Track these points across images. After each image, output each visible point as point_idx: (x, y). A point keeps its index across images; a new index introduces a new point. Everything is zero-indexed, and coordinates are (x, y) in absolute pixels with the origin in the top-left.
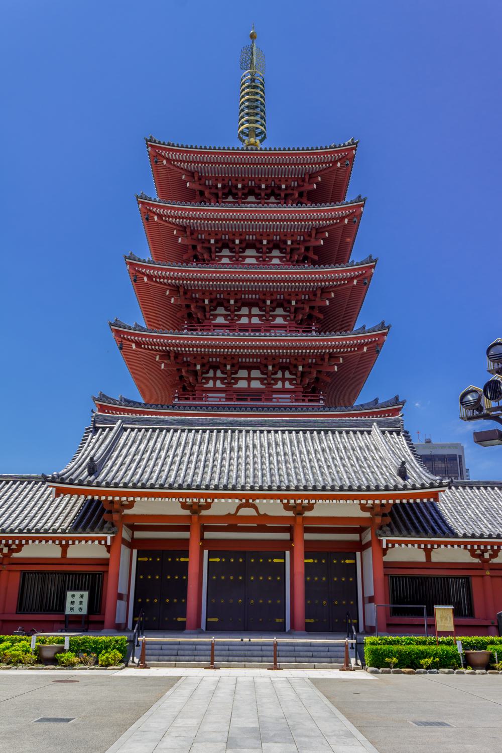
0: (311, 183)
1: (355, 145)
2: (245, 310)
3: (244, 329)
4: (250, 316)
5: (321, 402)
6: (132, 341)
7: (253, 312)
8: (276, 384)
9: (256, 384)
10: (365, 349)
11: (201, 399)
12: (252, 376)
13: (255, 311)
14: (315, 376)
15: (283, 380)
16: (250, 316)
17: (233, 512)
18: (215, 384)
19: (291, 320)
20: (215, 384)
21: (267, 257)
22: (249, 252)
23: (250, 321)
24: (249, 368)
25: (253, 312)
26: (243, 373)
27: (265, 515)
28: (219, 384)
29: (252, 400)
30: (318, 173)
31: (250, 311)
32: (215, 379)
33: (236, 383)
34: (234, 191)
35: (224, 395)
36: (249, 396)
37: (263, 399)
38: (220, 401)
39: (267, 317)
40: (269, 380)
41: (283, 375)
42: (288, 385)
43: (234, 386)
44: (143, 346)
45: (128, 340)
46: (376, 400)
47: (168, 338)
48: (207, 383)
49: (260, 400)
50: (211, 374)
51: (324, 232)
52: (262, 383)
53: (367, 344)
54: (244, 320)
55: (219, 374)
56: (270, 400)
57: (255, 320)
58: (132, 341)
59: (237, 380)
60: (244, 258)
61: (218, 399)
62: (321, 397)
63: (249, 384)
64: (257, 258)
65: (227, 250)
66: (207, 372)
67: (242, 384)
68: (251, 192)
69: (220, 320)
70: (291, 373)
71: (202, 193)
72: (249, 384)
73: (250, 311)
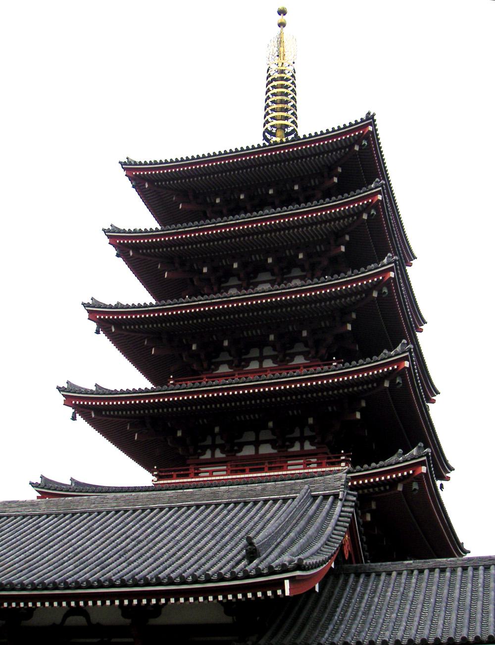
1: (370, 119)
2: (255, 352)
7: (265, 354)
8: (292, 446)
16: (261, 359)
17: (58, 621)
19: (313, 358)
20: (213, 454)
25: (265, 354)
26: (250, 436)
27: (98, 624)
28: (219, 454)
30: (337, 163)
31: (261, 352)
32: (213, 448)
33: (240, 450)
36: (249, 465)
37: (266, 469)
38: (211, 475)
40: (282, 442)
41: (302, 432)
42: (308, 446)
44: (104, 413)
49: (261, 470)
52: (273, 448)
59: (241, 447)
61: (208, 474)
62: (343, 458)
63: (257, 450)
65: (236, 278)
67: (248, 451)
71: (205, 213)
72: (257, 450)
73: (261, 352)
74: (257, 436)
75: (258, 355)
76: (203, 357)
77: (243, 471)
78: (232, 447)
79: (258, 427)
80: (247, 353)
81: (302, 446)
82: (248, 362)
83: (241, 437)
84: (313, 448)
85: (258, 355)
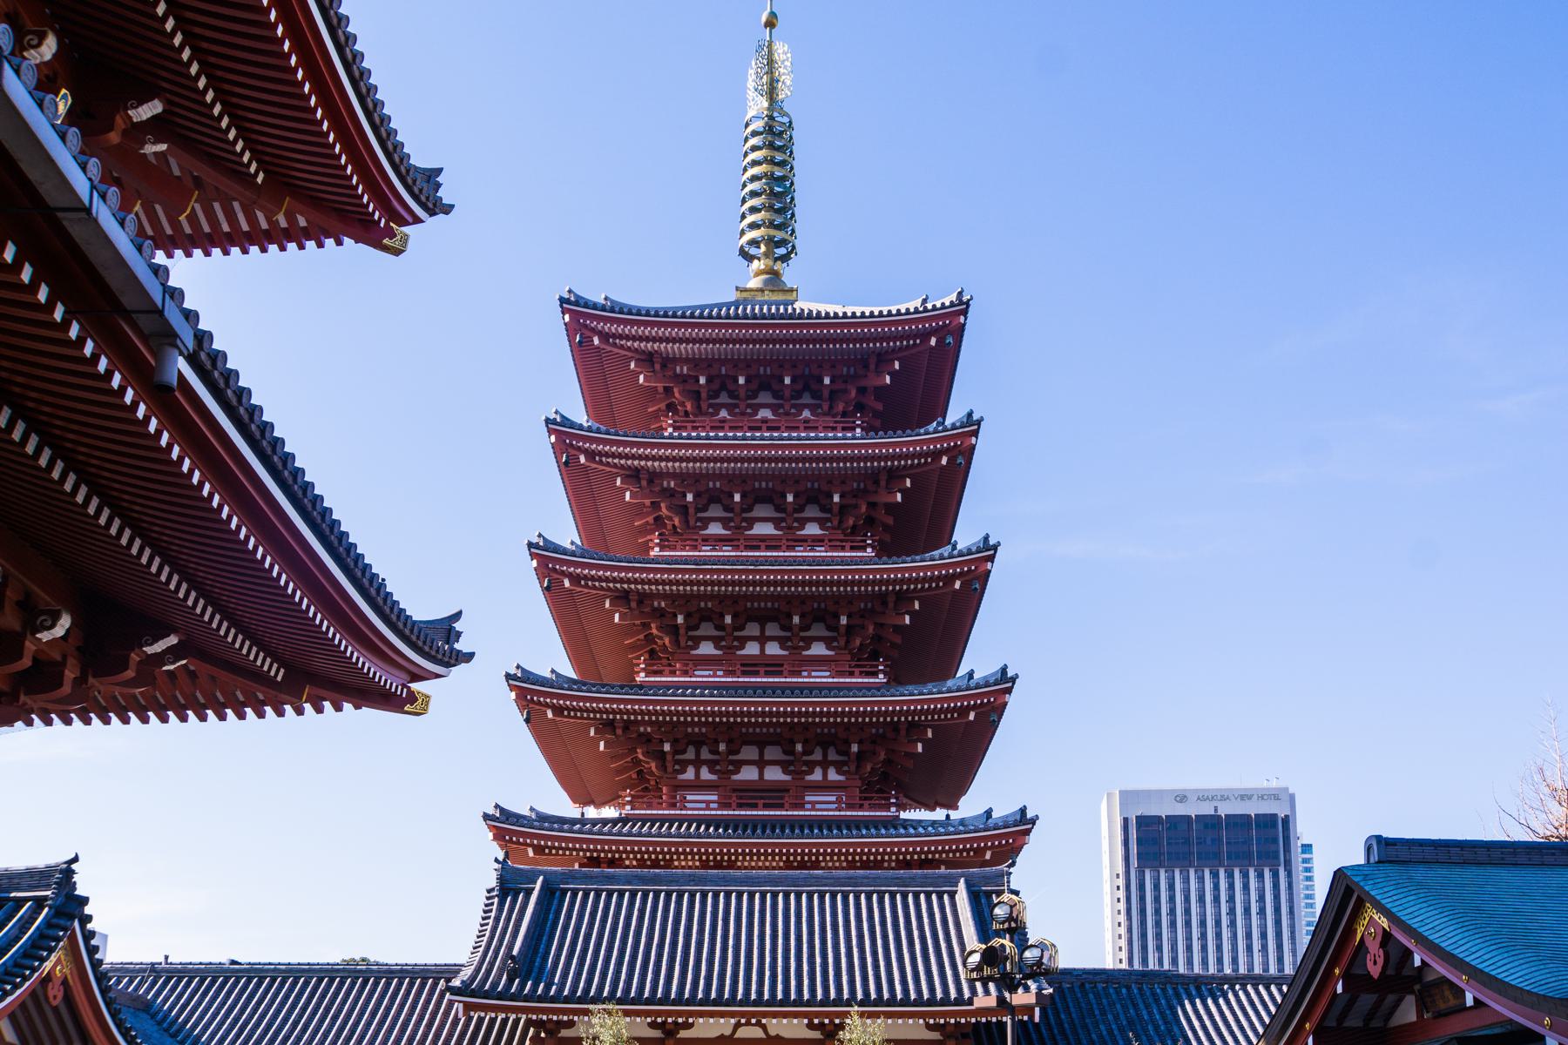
0: (879, 373)
2: (753, 629)
3: (751, 666)
6: (547, 706)
8: (811, 772)
9: (774, 774)
10: (972, 716)
11: (673, 806)
13: (772, 629)
14: (882, 756)
15: (825, 764)
16: (763, 640)
18: (697, 774)
20: (697, 774)
21: (796, 520)
22: (760, 511)
23: (762, 650)
24: (761, 743)
26: (749, 752)
28: (706, 775)
29: (766, 807)
31: (763, 630)
34: (731, 387)
35: (715, 798)
38: (708, 808)
41: (825, 755)
42: (833, 775)
43: (735, 777)
45: (539, 703)
46: (989, 813)
47: (605, 700)
49: (780, 807)
50: (690, 754)
51: (903, 478)
53: (974, 707)
54: (752, 649)
55: (705, 754)
56: (801, 806)
57: (773, 649)
58: (547, 706)
59: (738, 765)
60: (751, 522)
63: (761, 774)
64: (777, 523)
66: (684, 752)
67: (749, 774)
68: (764, 383)
69: (707, 649)
70: (838, 753)
72: (761, 774)
73: (763, 630)
74: (761, 754)
75: (757, 633)
77: (754, 807)
78: (726, 766)
81: (825, 775)
82: (743, 641)
84: (841, 778)
85: (757, 633)
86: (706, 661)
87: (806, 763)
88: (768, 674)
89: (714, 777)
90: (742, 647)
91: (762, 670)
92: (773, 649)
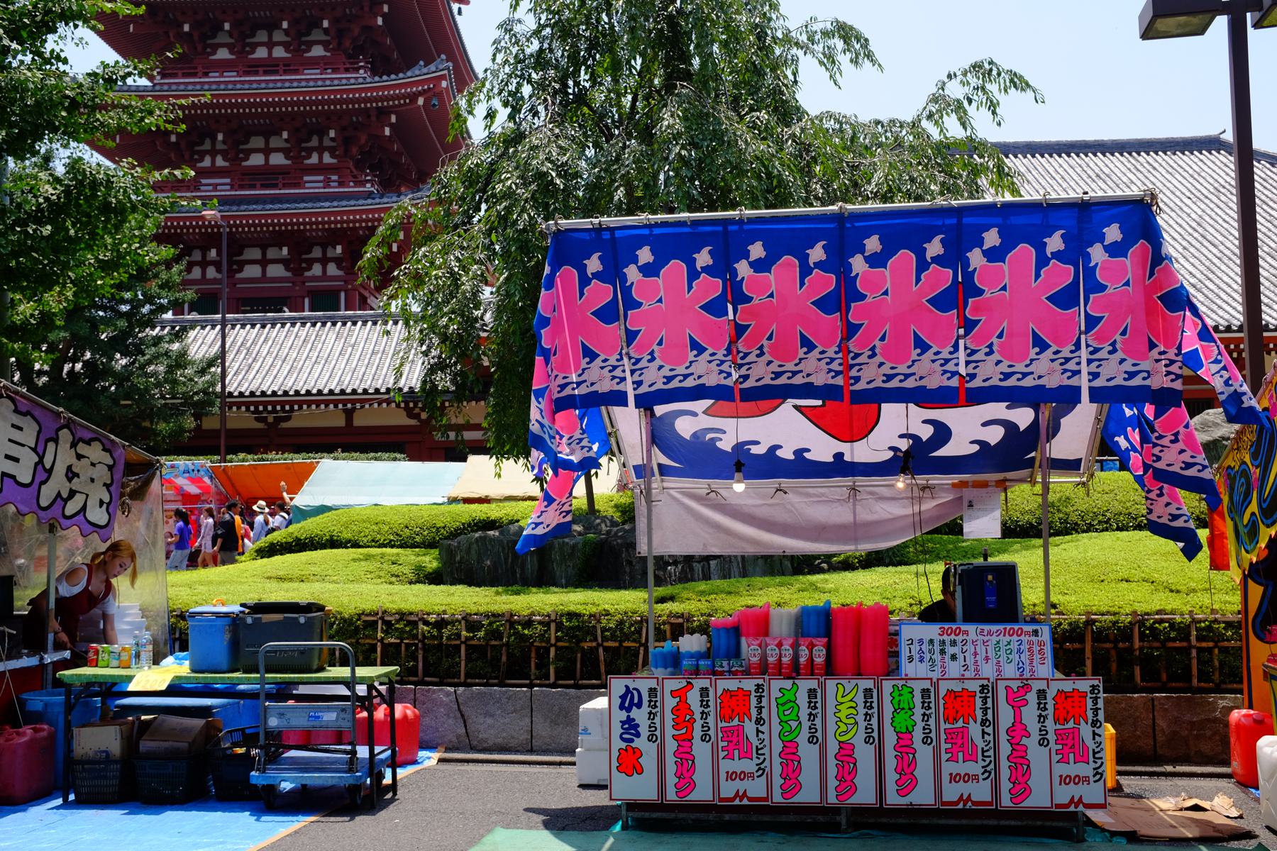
2: (262, 36)
4: (270, 45)
5: (368, 185)
9: (277, 159)
12: (272, 145)
18: (213, 161)
23: (270, 53)
28: (220, 162)
31: (270, 36)
35: (228, 181)
38: (215, 190)
39: (298, 43)
40: (296, 151)
41: (321, 141)
42: (327, 159)
43: (245, 164)
48: (202, 160)
49: (275, 186)
52: (287, 158)
54: (261, 53)
56: (297, 185)
57: (279, 52)
59: (248, 153)
63: (267, 159)
66: (202, 144)
67: (256, 160)
72: (267, 159)
74: (267, 143)
76: (196, 38)
77: (253, 187)
78: (236, 152)
79: (268, 133)
80: (253, 36)
81: (321, 158)
82: (255, 46)
83: (247, 142)
84: (334, 161)
86: (223, 66)
87: (306, 149)
88: (266, 73)
89: (226, 164)
90: (253, 52)
91: (261, 69)
92: (279, 52)
